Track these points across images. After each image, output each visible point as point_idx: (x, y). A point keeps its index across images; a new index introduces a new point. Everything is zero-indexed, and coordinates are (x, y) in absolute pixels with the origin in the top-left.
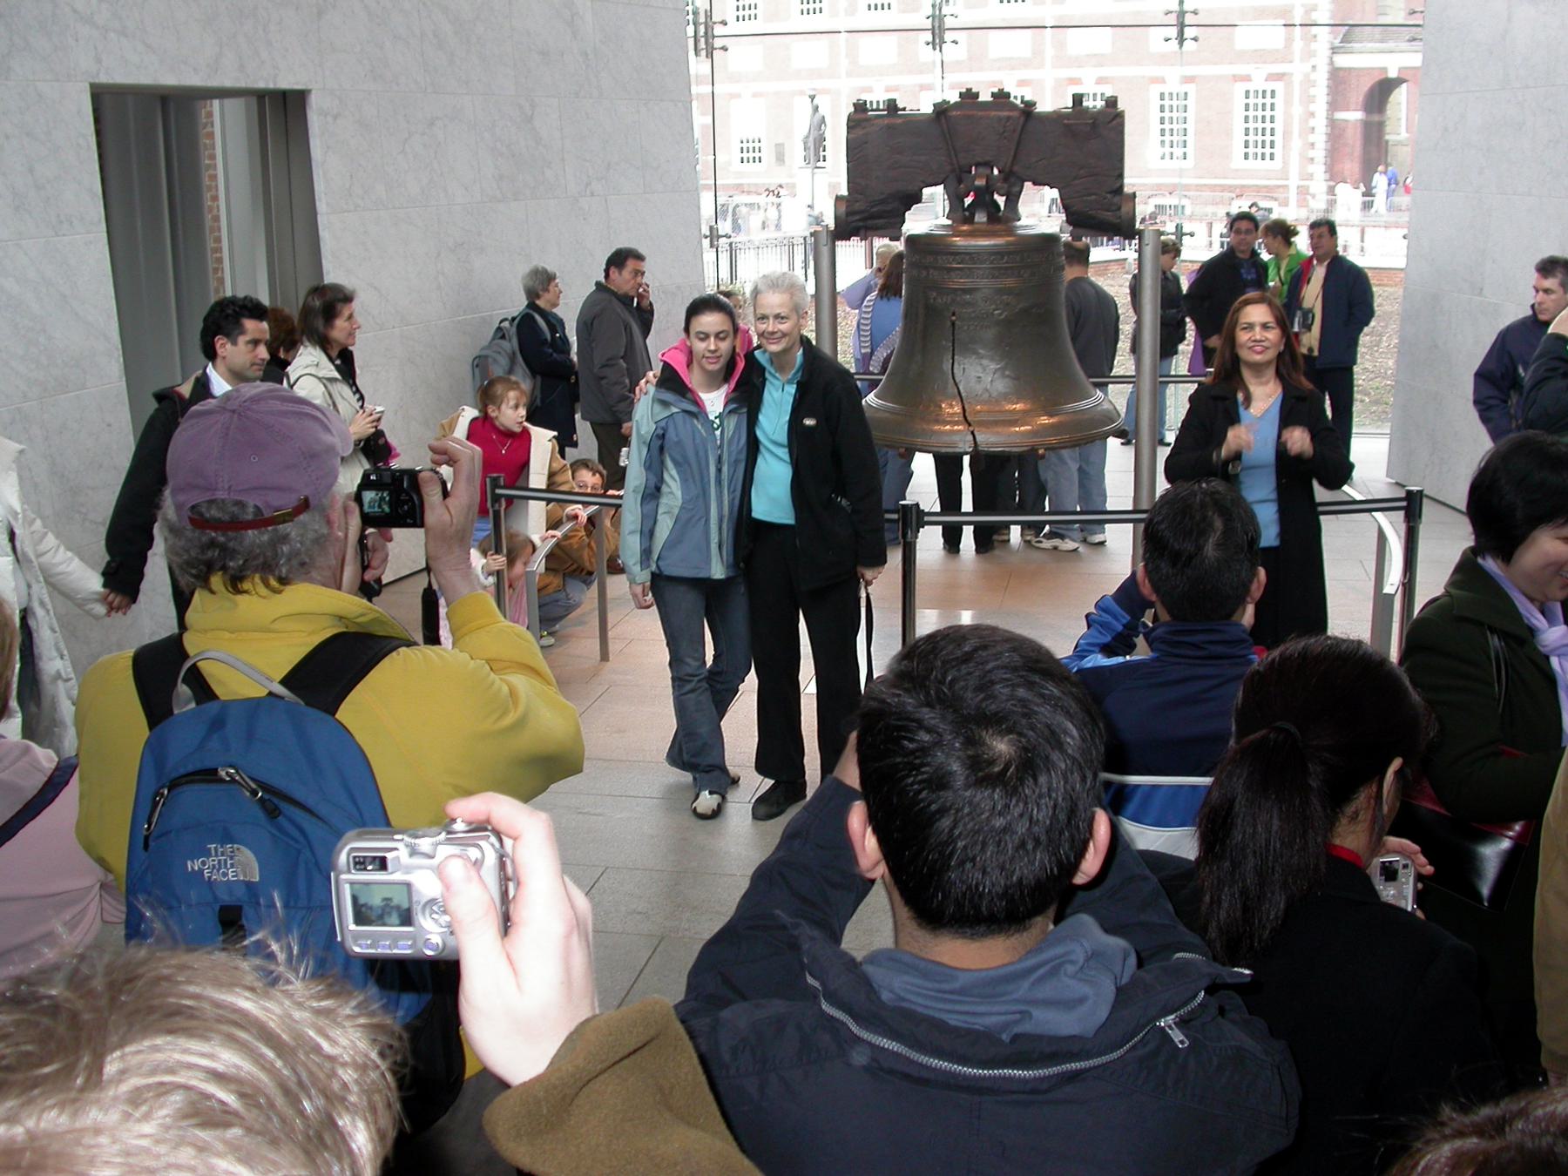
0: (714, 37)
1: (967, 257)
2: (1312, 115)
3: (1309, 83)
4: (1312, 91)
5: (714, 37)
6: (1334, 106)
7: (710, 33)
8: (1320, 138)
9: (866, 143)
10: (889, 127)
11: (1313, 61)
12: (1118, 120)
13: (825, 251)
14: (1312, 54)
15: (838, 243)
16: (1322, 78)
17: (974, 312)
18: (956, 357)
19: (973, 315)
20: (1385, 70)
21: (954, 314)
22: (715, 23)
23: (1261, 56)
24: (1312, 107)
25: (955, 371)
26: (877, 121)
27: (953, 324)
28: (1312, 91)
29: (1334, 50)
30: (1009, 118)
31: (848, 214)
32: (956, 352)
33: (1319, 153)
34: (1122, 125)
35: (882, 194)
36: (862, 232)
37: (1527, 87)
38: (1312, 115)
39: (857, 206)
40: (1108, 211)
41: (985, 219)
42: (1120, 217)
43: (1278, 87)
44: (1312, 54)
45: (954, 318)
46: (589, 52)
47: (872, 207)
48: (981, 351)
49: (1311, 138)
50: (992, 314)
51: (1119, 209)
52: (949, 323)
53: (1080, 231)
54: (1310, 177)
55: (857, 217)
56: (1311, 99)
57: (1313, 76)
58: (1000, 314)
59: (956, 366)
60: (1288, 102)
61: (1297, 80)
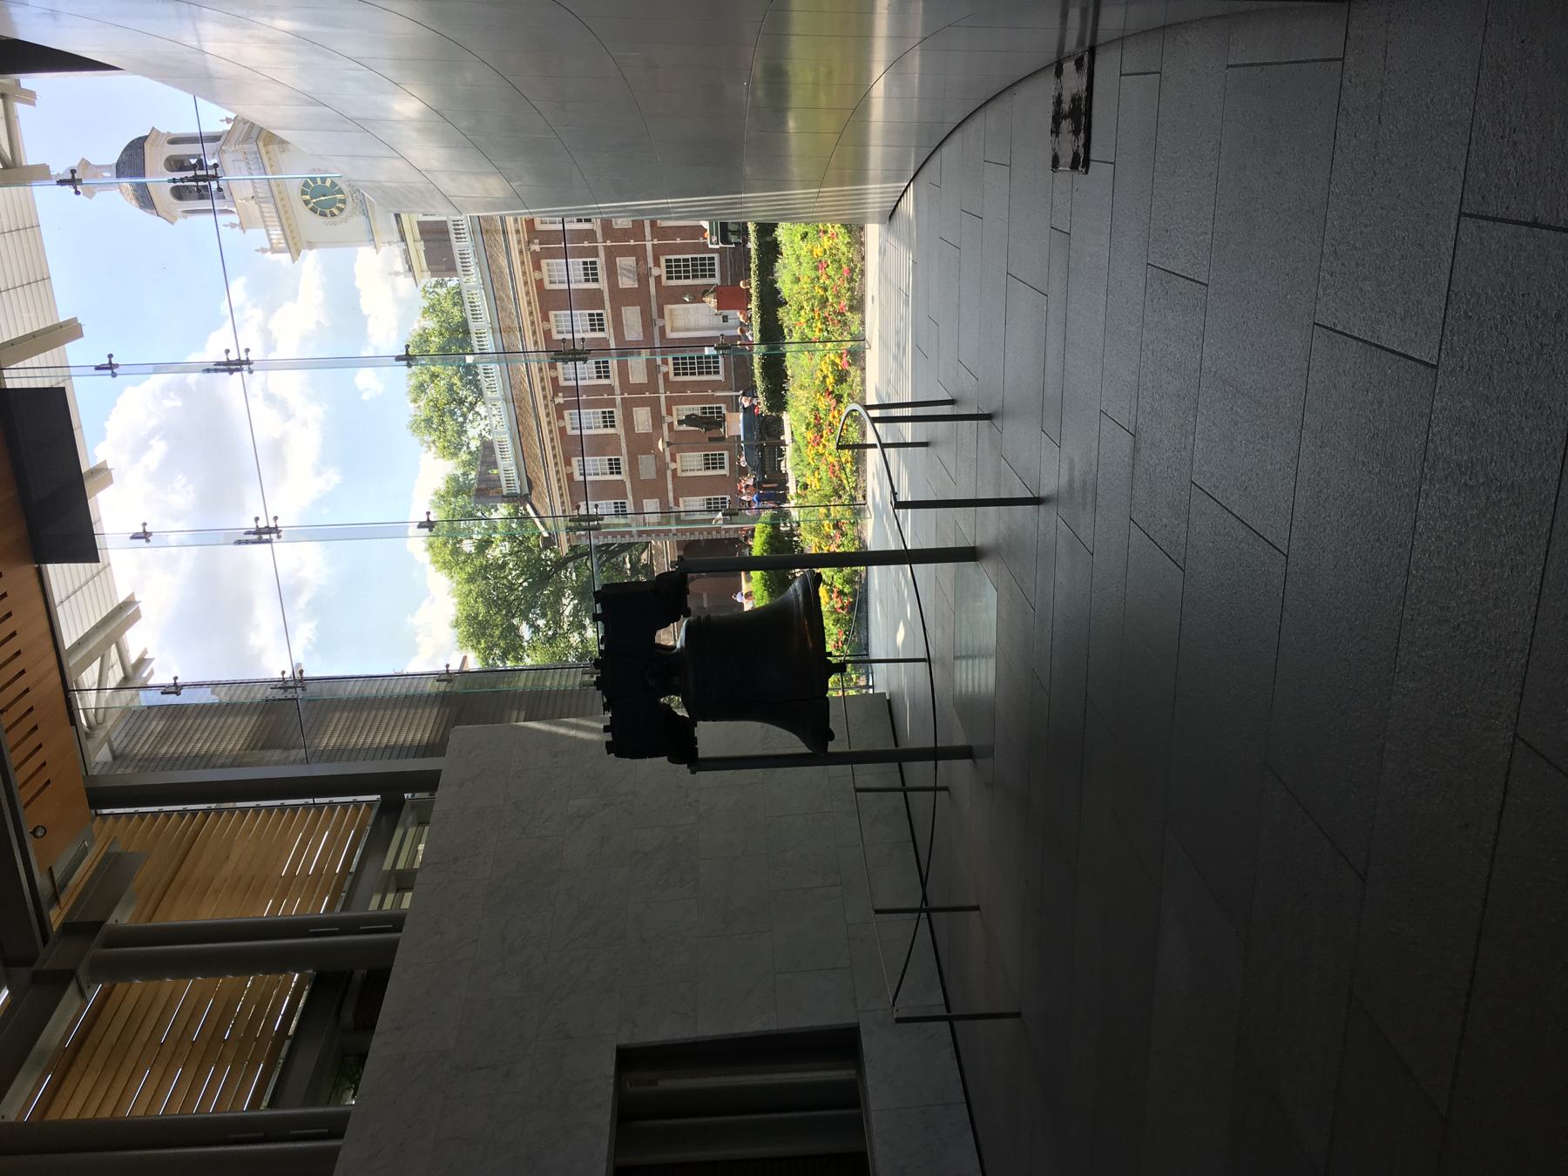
15: (700, 756)
46: (602, 803)
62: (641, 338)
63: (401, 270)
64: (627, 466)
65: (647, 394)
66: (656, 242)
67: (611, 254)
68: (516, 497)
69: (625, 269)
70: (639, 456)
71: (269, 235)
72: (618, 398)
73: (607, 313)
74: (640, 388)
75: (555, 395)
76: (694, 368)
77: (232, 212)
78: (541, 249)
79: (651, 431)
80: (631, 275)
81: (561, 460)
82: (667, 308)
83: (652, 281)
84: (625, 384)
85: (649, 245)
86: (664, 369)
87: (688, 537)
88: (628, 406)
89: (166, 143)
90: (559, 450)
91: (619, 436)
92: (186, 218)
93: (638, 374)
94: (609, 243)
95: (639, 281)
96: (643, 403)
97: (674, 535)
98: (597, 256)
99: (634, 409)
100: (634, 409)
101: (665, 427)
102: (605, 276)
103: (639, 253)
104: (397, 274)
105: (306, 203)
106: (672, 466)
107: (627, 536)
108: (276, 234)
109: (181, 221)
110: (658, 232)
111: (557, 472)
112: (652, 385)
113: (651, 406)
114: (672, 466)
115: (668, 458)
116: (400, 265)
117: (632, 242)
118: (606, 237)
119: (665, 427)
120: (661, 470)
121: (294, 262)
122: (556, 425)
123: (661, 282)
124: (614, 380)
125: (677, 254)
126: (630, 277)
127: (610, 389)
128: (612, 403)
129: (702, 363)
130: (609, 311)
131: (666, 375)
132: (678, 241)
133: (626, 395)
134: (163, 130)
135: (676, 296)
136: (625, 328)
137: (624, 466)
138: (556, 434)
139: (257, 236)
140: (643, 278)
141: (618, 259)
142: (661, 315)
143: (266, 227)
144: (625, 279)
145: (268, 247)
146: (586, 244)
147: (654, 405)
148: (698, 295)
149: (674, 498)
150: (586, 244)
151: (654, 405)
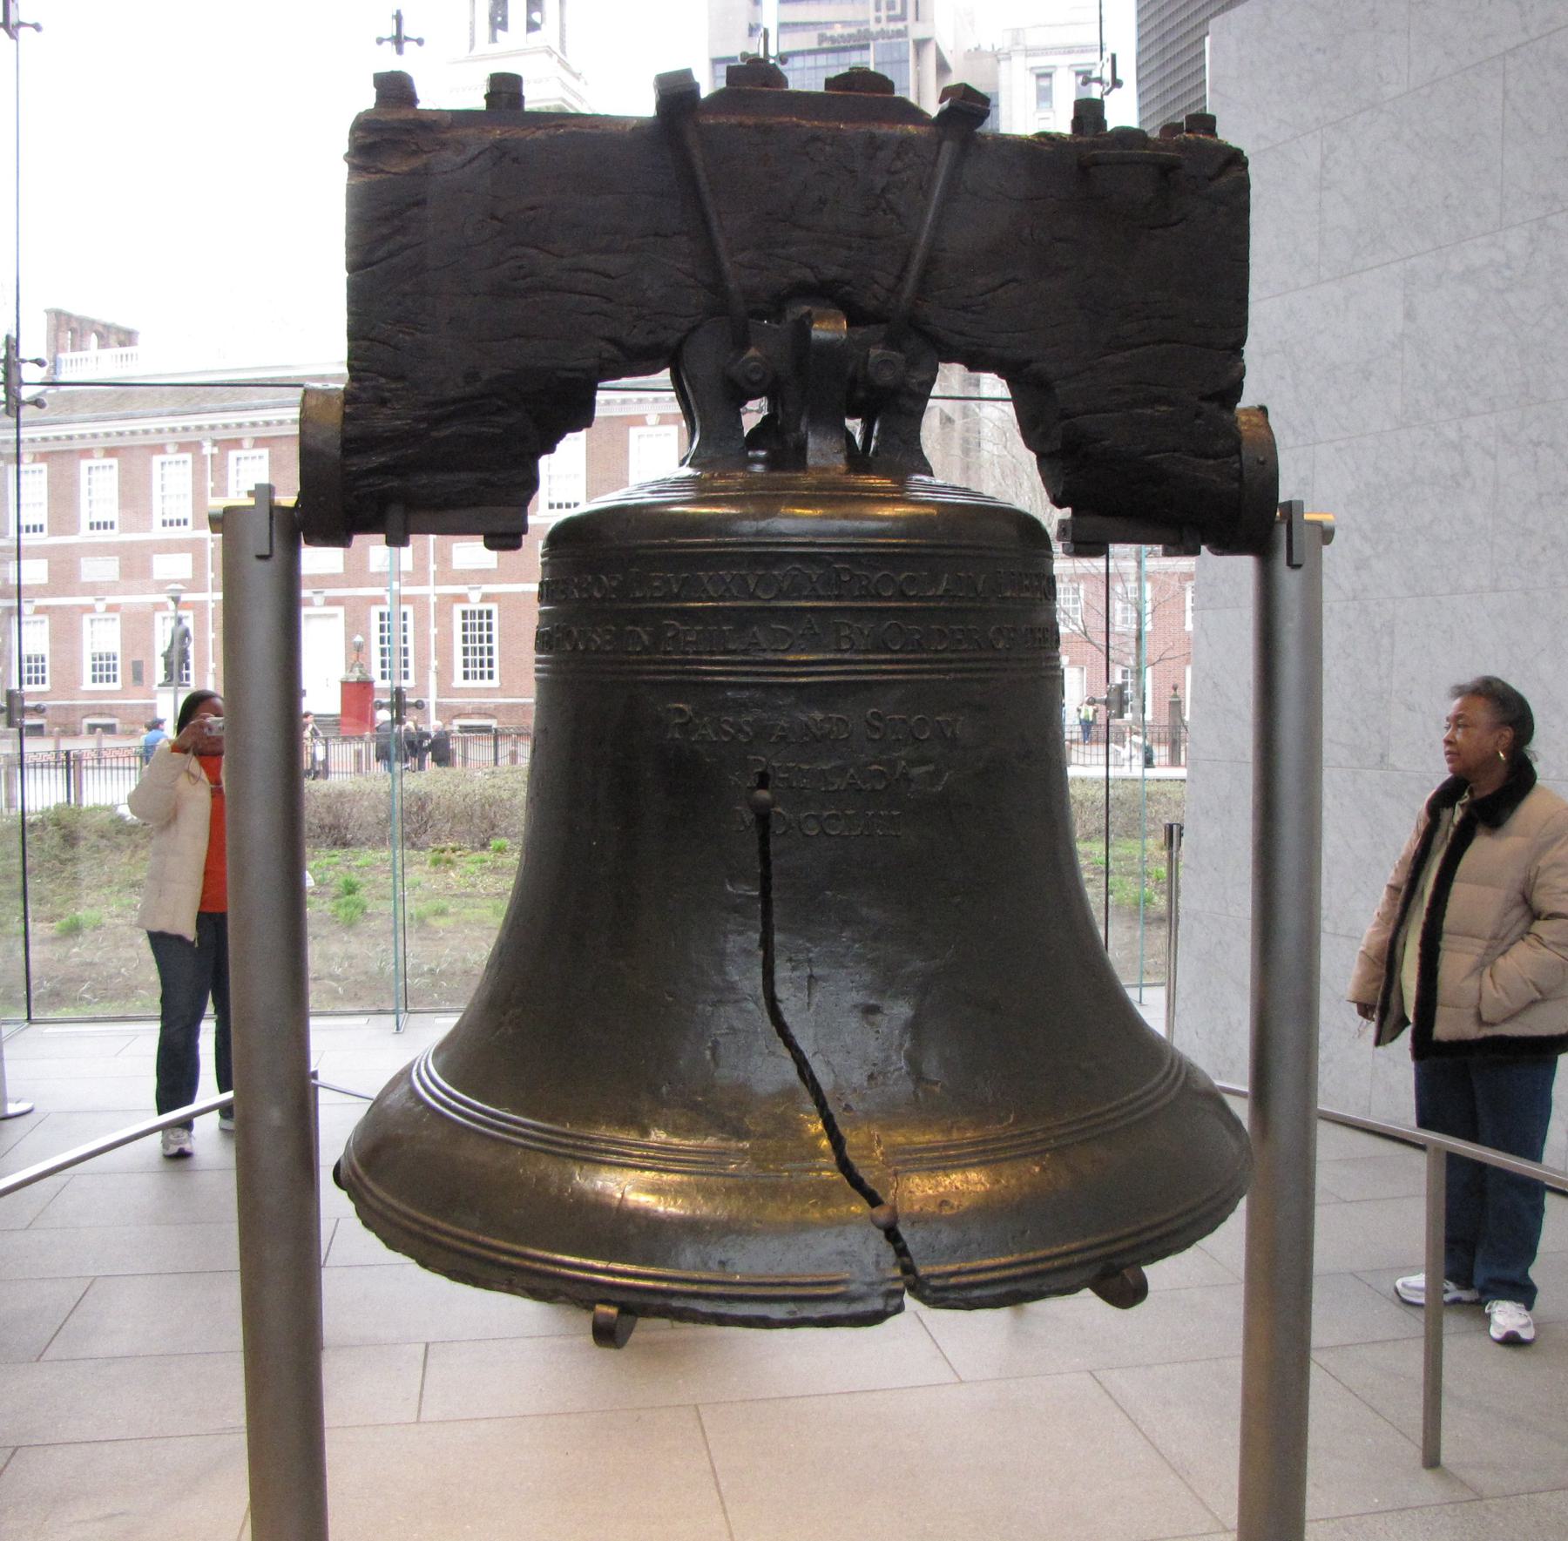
0: (21, 383)
1: (815, 572)
5: (21, 383)
7: (14, 379)
9: (420, 203)
10: (500, 152)
12: (1234, 173)
13: (262, 577)
17: (842, 770)
18: (778, 938)
19: (839, 783)
21: (764, 781)
22: (24, 361)
25: (782, 992)
26: (460, 133)
27: (763, 818)
30: (906, 143)
31: (353, 444)
32: (777, 910)
34: (1244, 186)
35: (471, 377)
36: (395, 515)
37: (1468, 414)
39: (383, 421)
40: (1207, 457)
41: (840, 462)
42: (1239, 477)
45: (764, 795)
47: (437, 422)
48: (864, 911)
50: (905, 775)
51: (1237, 451)
52: (749, 817)
53: (1092, 521)
55: (376, 460)
58: (936, 776)
59: (782, 971)
66: (433, 600)
70: (117, 558)
75: (215, 443)
77: (472, 47)
81: (115, 442)
82: (340, 610)
83: (378, 591)
85: (431, 591)
91: (149, 532)
95: (380, 574)
106: (100, 607)
110: (446, 602)
114: (100, 607)
122: (168, 439)
123: (376, 604)
132: (433, 631)
135: (355, 623)
137: (102, 536)
138: (155, 440)
140: (379, 579)
142: (330, 602)
148: (357, 652)
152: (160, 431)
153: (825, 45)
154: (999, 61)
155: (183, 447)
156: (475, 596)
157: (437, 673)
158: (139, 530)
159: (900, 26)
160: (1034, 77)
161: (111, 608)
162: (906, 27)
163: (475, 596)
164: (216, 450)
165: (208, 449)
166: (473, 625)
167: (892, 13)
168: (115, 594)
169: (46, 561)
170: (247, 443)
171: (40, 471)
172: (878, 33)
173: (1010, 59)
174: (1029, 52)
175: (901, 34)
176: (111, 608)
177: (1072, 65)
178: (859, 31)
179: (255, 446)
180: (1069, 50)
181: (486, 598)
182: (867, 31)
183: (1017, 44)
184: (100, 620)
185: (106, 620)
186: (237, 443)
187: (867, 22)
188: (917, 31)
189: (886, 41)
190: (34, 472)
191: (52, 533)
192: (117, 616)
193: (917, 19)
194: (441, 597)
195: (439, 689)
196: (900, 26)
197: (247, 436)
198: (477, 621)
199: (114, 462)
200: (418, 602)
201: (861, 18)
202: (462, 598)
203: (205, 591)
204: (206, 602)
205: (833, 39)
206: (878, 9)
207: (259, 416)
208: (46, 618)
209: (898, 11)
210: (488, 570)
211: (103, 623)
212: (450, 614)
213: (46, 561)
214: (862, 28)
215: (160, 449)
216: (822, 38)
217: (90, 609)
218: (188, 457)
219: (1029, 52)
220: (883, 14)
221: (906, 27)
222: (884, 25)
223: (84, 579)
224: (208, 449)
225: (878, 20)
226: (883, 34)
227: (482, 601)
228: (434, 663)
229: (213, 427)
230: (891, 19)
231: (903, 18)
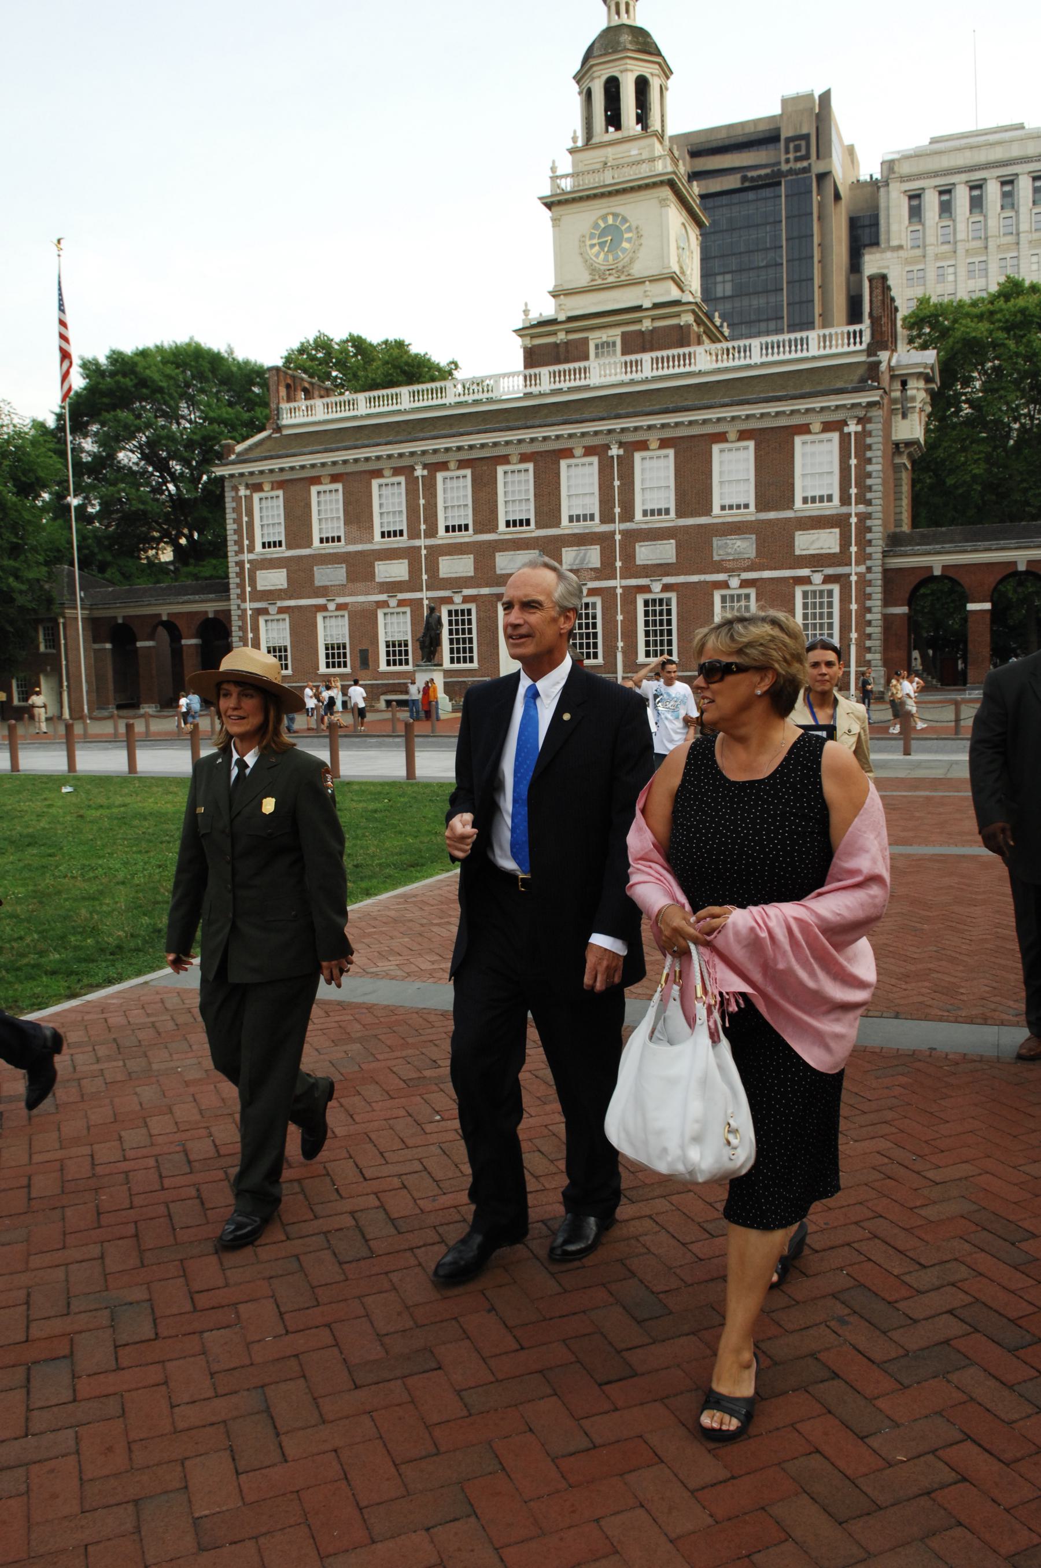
2: (869, 610)
3: (863, 582)
4: (868, 590)
6: (887, 602)
8: (876, 630)
11: (869, 563)
14: (870, 557)
16: (876, 577)
20: (930, 568)
23: (817, 561)
24: (868, 603)
28: (868, 590)
29: (885, 554)
33: (875, 643)
38: (869, 610)
43: (836, 588)
44: (870, 557)
49: (869, 630)
54: (868, 664)
56: (869, 597)
57: (869, 576)
60: (845, 599)
61: (854, 578)
62: (498, 572)
63: (530, 317)
64: (331, 551)
65: (425, 577)
66: (619, 591)
67: (604, 540)
68: (278, 419)
69: (585, 555)
70: (344, 565)
71: (566, 176)
72: (422, 542)
73: (532, 531)
74: (433, 569)
75: (425, 466)
76: (457, 633)
78: (612, 457)
79: (377, 580)
80: (577, 562)
81: (339, 469)
84: (436, 552)
85: (617, 583)
86: (458, 599)
87: (236, 623)
88: (411, 554)
89: (660, 82)
90: (350, 468)
92: (580, 93)
93: (452, 567)
94: (618, 537)
96: (414, 570)
97: (239, 606)
98: (603, 521)
99: (406, 561)
100: (406, 561)
101: (383, 597)
102: (576, 531)
103: (606, 570)
104: (526, 312)
105: (604, 218)
106: (332, 606)
107: (236, 548)
108: (567, 184)
109: (576, 88)
110: (631, 593)
111: (323, 465)
112: (436, 582)
113: (410, 581)
114: (332, 606)
115: (341, 600)
116: (534, 316)
117: (618, 564)
118: (625, 533)
119: (383, 597)
120: (323, 591)
121: (540, 199)
124: (442, 537)
125: (603, 615)
126: (575, 559)
127: (432, 532)
128: (414, 534)
129: (464, 643)
130: (533, 535)
131: (449, 600)
132: (620, 617)
133: (424, 552)
134: (671, 83)
136: (512, 553)
137: (331, 548)
139: (566, 165)
141: (598, 547)
143: (572, 175)
144: (573, 554)
145: (558, 173)
146: (617, 510)
147: (413, 584)
149: (289, 607)
150: (617, 510)
151: (413, 584)
152: (378, 458)
153: (747, 184)
154: (878, 188)
155: (397, 471)
156: (657, 587)
157: (624, 653)
158: (361, 542)
159: (805, 164)
160: (906, 199)
161: (340, 607)
162: (810, 164)
163: (657, 587)
164: (425, 472)
165: (419, 472)
166: (654, 611)
167: (798, 154)
168: (344, 595)
169: (285, 570)
170: (452, 465)
171: (277, 497)
172: (788, 171)
173: (887, 185)
174: (904, 179)
175: (807, 170)
176: (340, 607)
177: (936, 187)
178: (773, 171)
179: (459, 468)
180: (936, 174)
181: (666, 588)
182: (779, 170)
183: (894, 173)
184: (331, 617)
185: (336, 617)
186: (444, 466)
187: (779, 163)
188: (818, 168)
189: (794, 177)
190: (272, 498)
191: (289, 547)
192: (346, 613)
193: (818, 157)
194: (625, 588)
195: (625, 666)
196: (805, 164)
197: (453, 458)
198: (658, 608)
199: (339, 486)
200: (607, 594)
201: (772, 161)
202: (646, 589)
203: (422, 590)
204: (422, 599)
205: (752, 179)
206: (787, 152)
207: (465, 441)
208: (286, 616)
209: (803, 152)
210: (668, 564)
211: (333, 619)
212: (634, 602)
213: (285, 570)
214: (776, 169)
215: (378, 473)
216: (744, 179)
217: (324, 608)
218: (402, 479)
219: (904, 179)
220: (791, 156)
221: (810, 164)
222: (791, 165)
223: (317, 583)
224: (419, 472)
225: (787, 161)
226: (791, 172)
227: (662, 591)
228: (620, 644)
229: (424, 452)
230: (797, 159)
231: (807, 157)
